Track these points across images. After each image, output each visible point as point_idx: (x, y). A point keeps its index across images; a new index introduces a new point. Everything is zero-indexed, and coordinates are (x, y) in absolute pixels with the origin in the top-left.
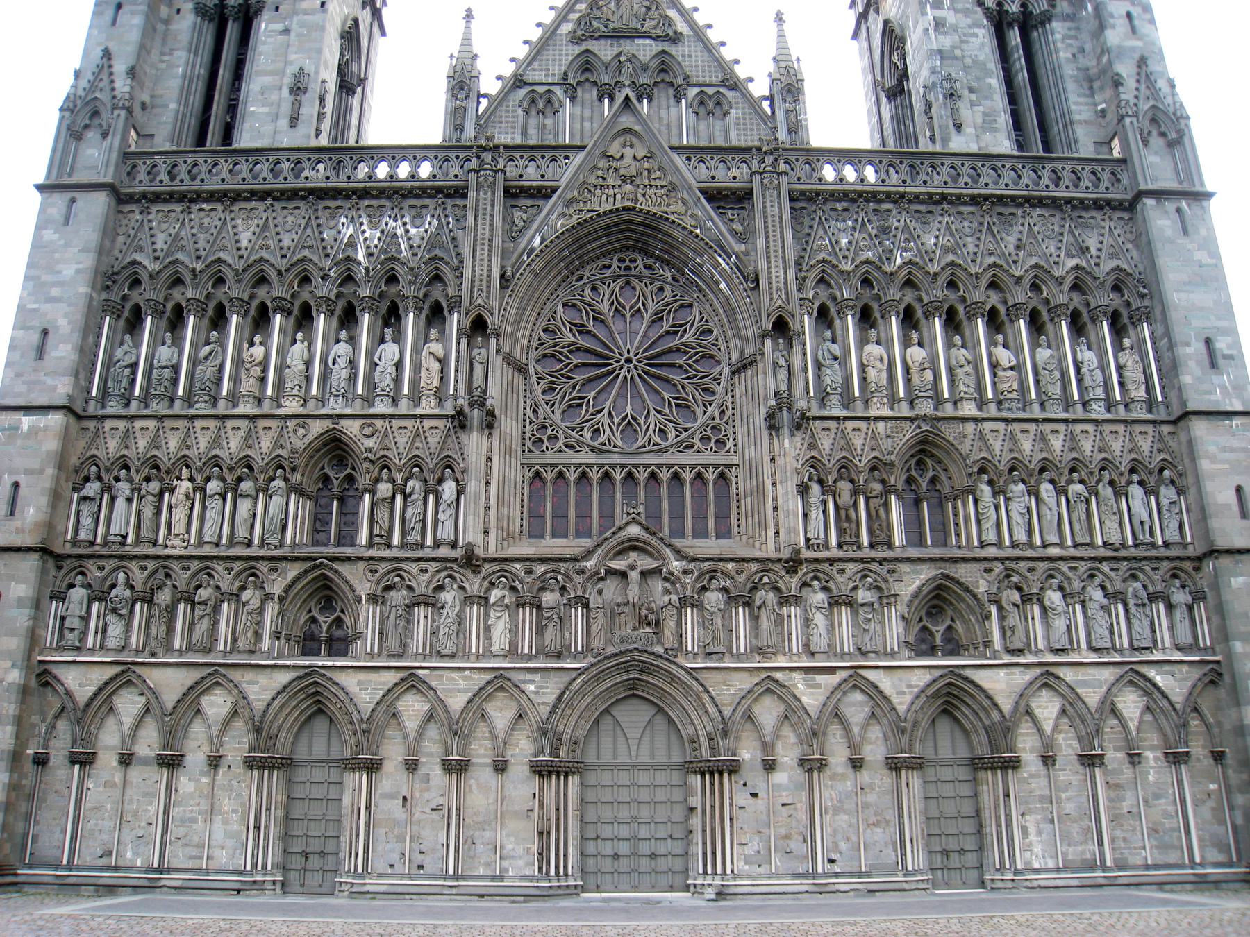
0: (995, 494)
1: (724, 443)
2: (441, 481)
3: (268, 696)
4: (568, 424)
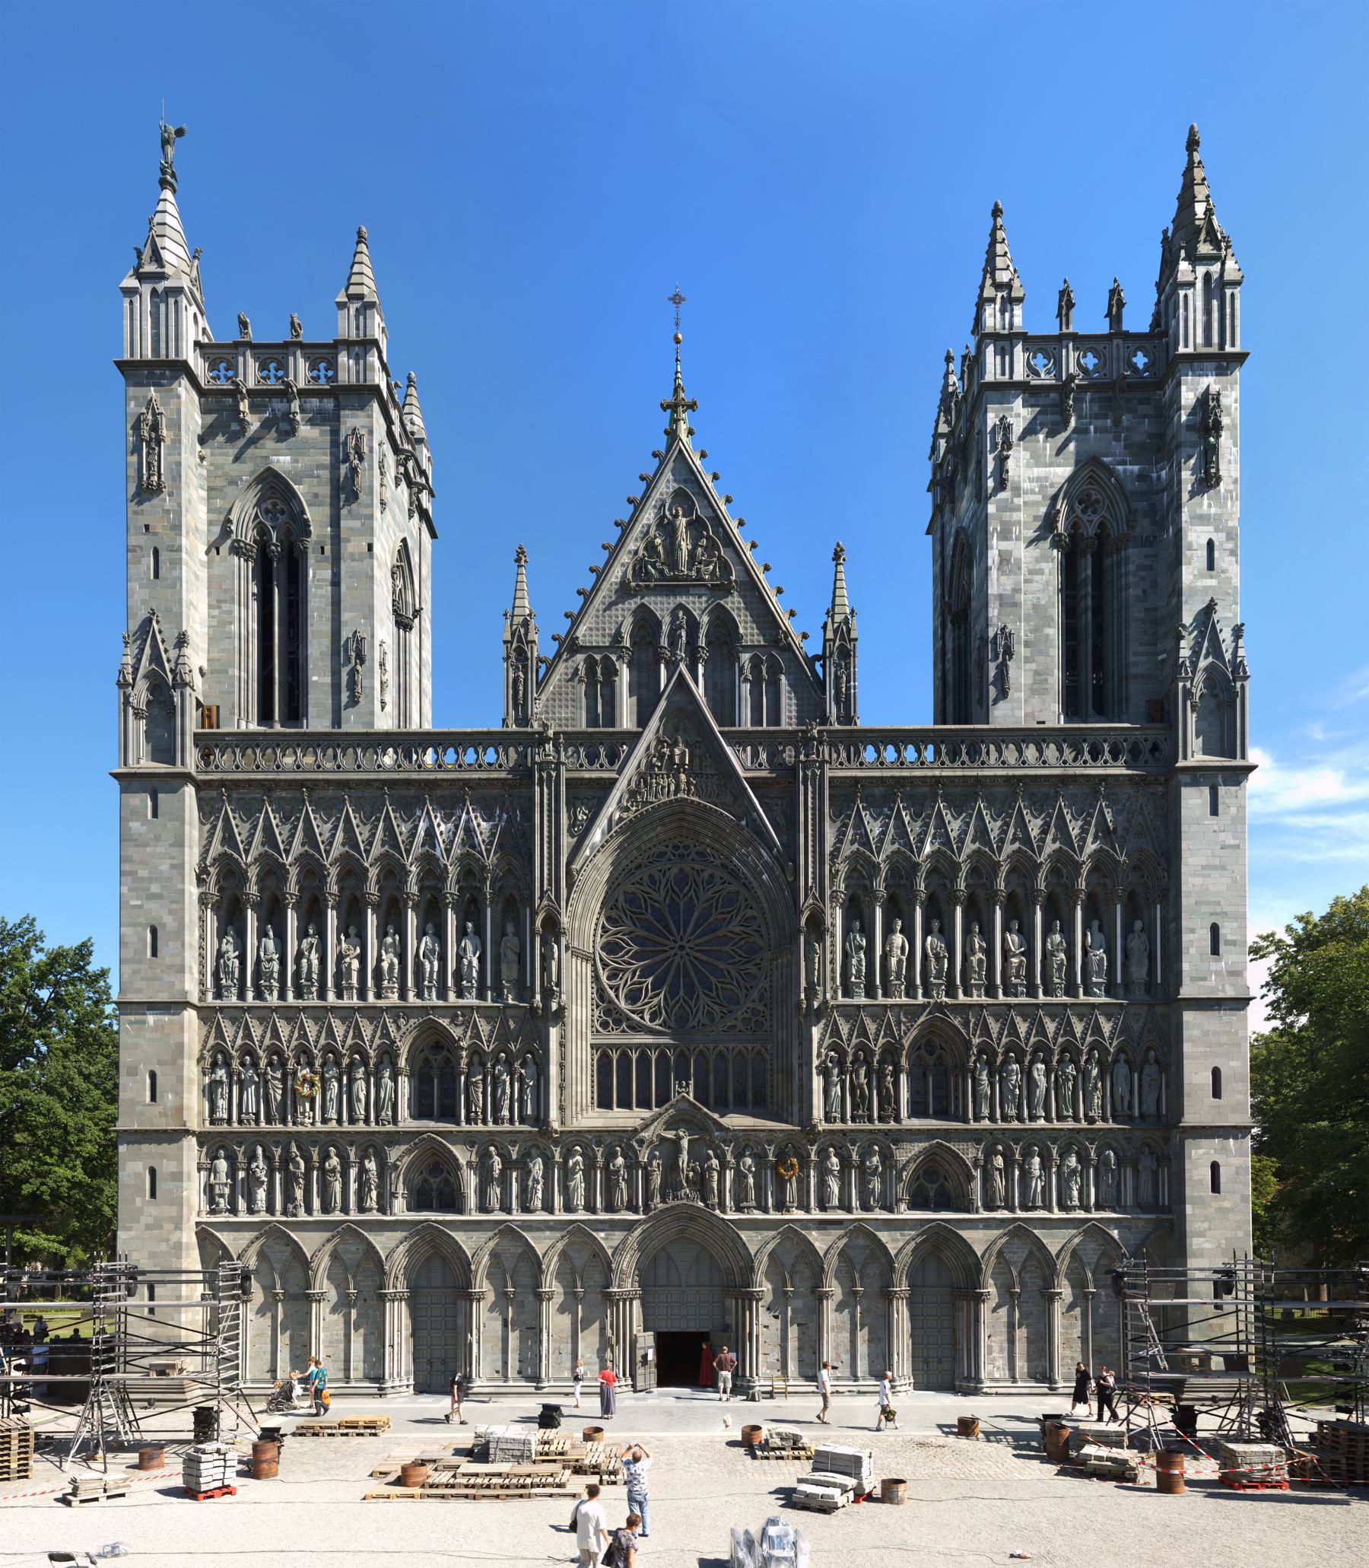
0: (991, 1075)
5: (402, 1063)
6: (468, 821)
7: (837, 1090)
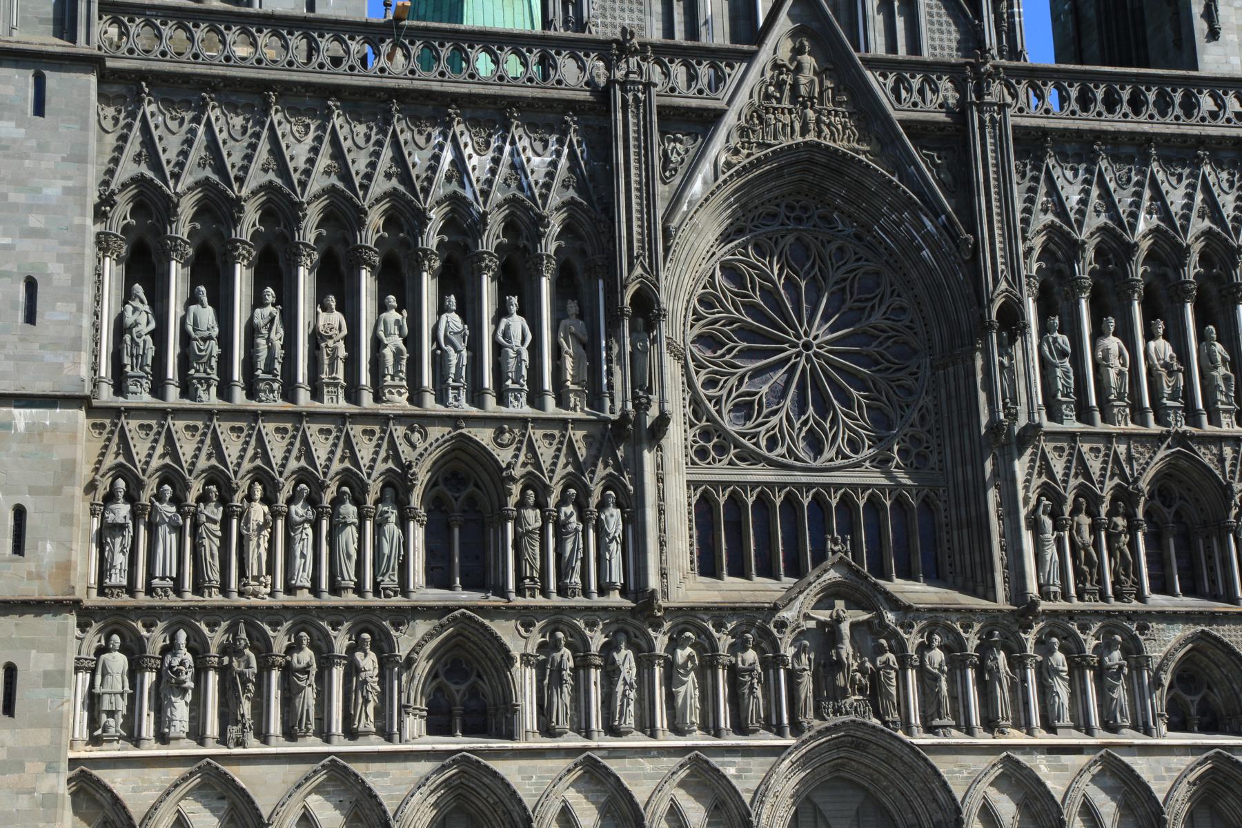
1: (926, 458)
2: (602, 506)
3: (403, 791)
4: (737, 428)
5: (415, 500)
6: (515, 153)
7: (1051, 552)
